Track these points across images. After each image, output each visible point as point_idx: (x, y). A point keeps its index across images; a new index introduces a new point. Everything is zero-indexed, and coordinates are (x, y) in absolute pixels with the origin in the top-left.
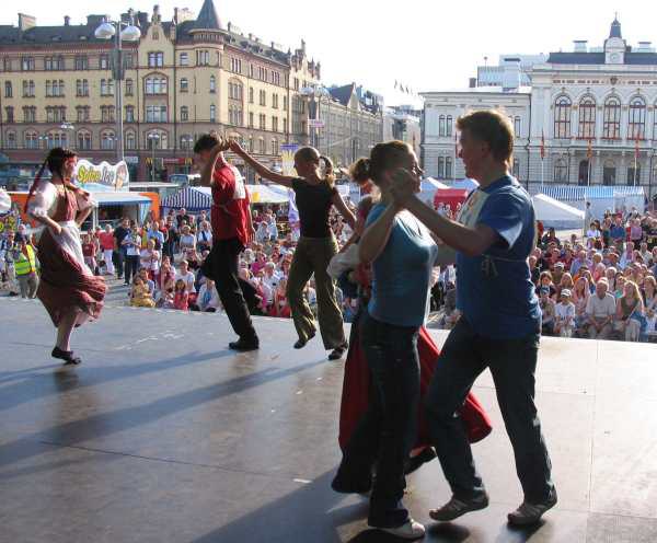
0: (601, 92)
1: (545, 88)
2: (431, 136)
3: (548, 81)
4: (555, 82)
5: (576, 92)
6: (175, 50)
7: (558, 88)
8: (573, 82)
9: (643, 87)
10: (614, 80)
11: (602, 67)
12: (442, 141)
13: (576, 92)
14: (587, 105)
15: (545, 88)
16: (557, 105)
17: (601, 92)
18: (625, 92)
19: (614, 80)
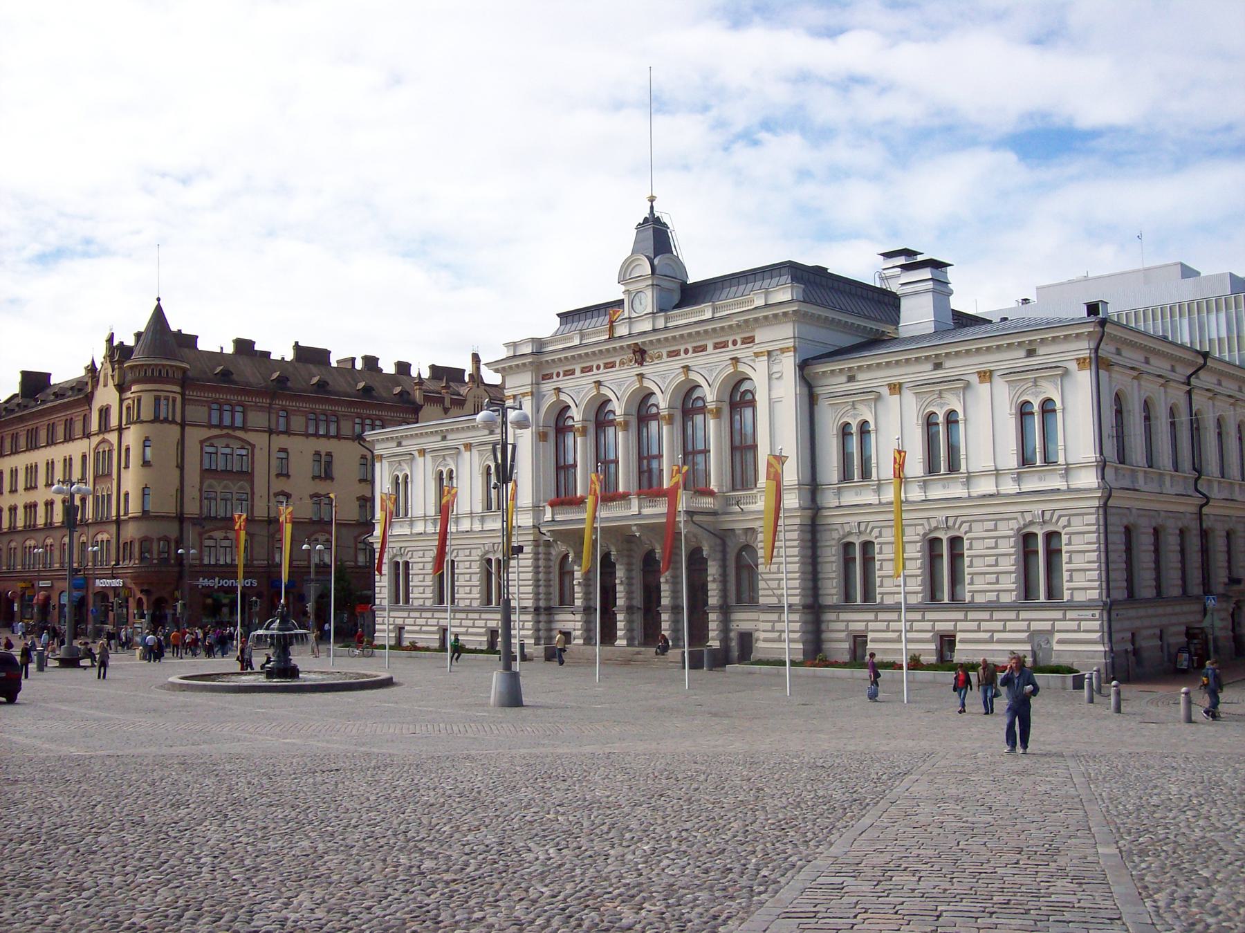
0: (619, 385)
5: (577, 393)
6: (121, 401)
10: (640, 354)
13: (577, 393)
17: (619, 385)
19: (640, 354)
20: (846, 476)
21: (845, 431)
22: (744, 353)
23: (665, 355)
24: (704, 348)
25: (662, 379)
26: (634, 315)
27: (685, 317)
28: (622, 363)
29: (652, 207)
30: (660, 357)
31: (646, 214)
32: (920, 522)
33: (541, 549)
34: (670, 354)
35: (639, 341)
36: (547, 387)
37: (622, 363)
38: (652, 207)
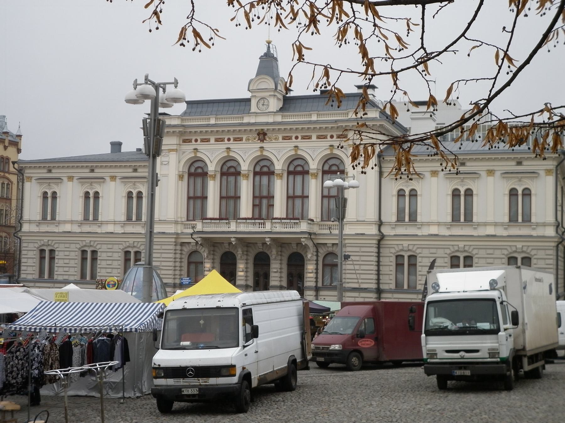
0: (246, 154)
2: (30, 222)
4: (185, 141)
5: (212, 156)
7: (188, 152)
8: (208, 140)
10: (262, 135)
13: (212, 156)
14: (230, 170)
17: (246, 154)
18: (279, 153)
19: (262, 135)
20: (400, 219)
21: (401, 194)
24: (310, 137)
25: (279, 153)
26: (259, 111)
27: (292, 118)
28: (248, 139)
29: (269, 47)
31: (265, 50)
33: (179, 247)
34: (284, 138)
35: (265, 128)
36: (188, 148)
37: (248, 139)
38: (269, 47)
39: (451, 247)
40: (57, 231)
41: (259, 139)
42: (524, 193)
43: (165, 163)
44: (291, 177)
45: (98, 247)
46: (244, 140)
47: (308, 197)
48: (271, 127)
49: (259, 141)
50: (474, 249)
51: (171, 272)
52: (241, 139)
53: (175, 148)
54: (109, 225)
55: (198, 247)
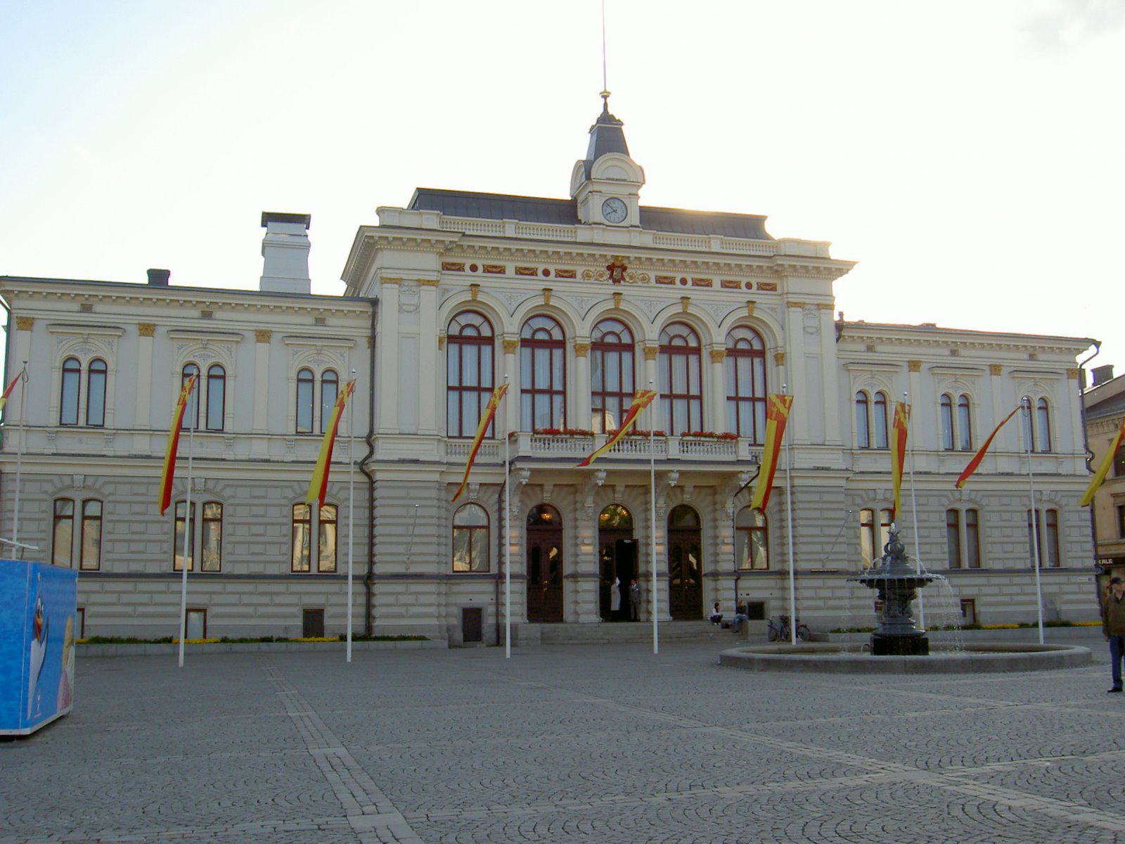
0: (582, 306)
1: (421, 283)
3: (429, 262)
4: (447, 267)
5: (510, 303)
9: (697, 294)
10: (616, 270)
11: (583, 234)
12: (69, 443)
13: (510, 303)
15: (421, 283)
16: (451, 339)
19: (616, 270)
22: (763, 299)
23: (653, 280)
28: (587, 275)
30: (645, 279)
32: (945, 493)
34: (660, 280)
35: (633, 254)
37: (587, 275)
39: (56, 479)
40: (111, 453)
41: (611, 277)
42: (325, 378)
43: (412, 308)
44: (599, 354)
45: (228, 492)
46: (579, 276)
47: (594, 394)
48: (644, 255)
49: (611, 281)
50: (106, 483)
51: (401, 549)
52: (572, 275)
53: (434, 278)
54: (254, 441)
55: (480, 495)
